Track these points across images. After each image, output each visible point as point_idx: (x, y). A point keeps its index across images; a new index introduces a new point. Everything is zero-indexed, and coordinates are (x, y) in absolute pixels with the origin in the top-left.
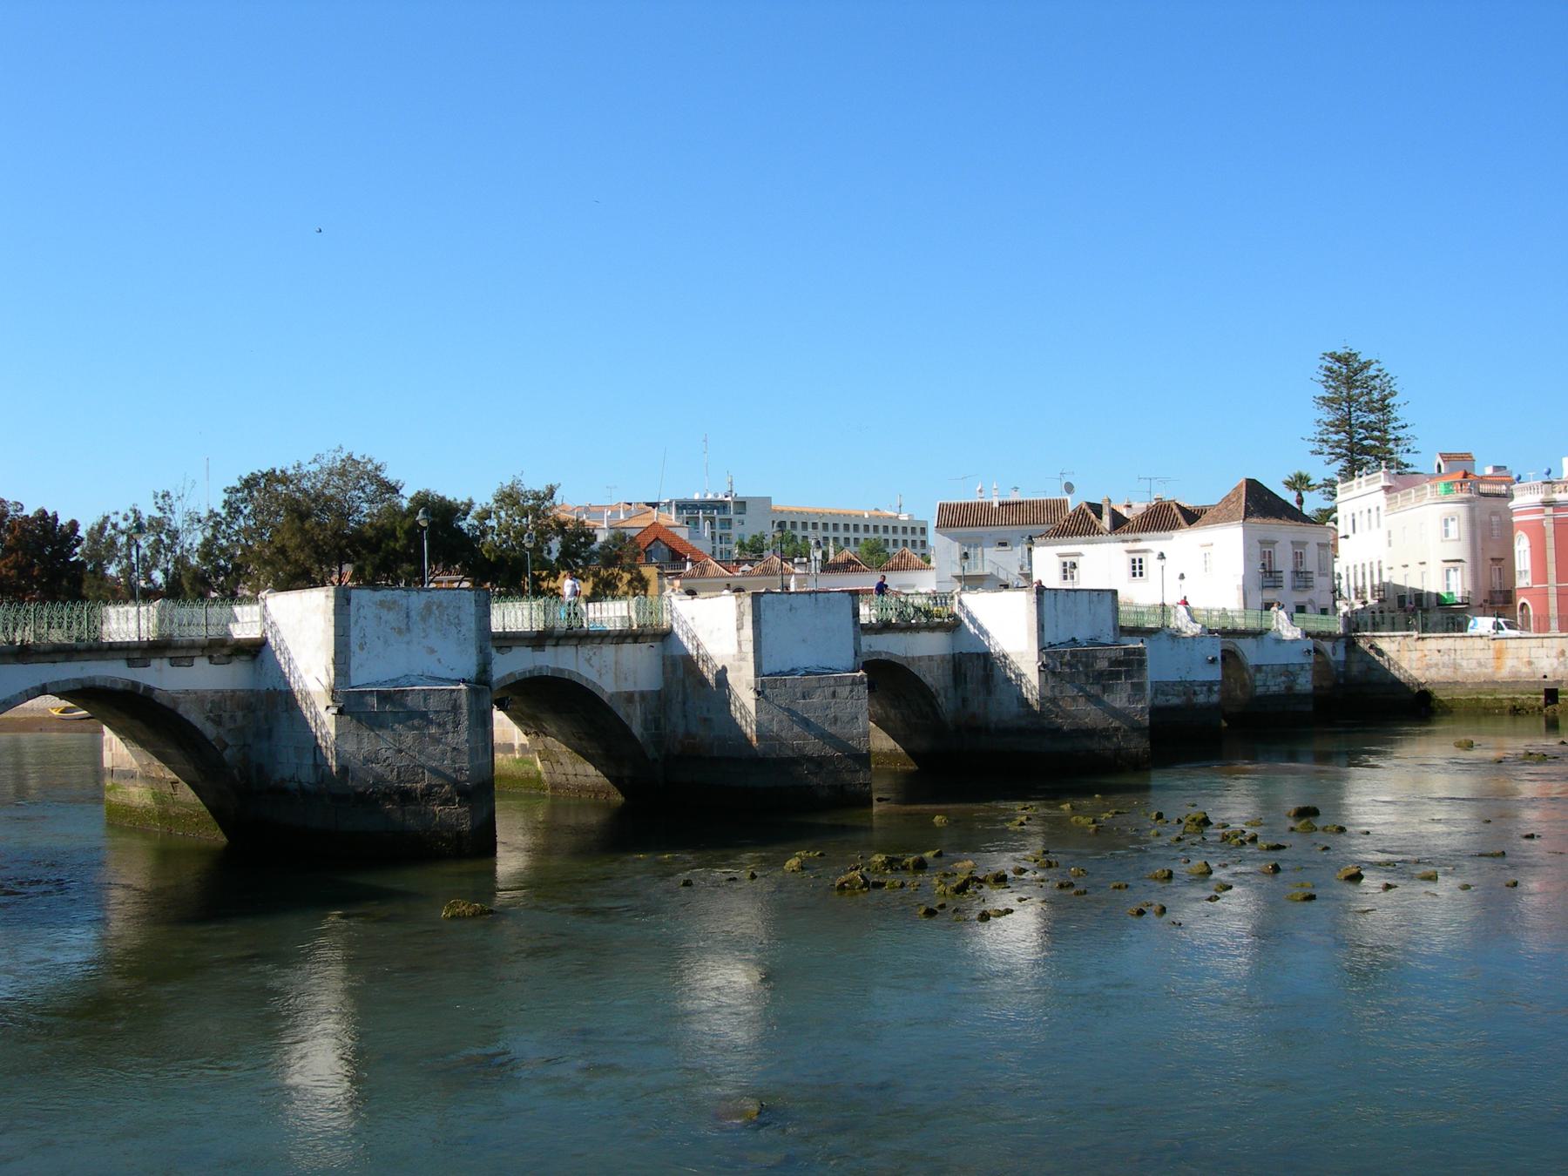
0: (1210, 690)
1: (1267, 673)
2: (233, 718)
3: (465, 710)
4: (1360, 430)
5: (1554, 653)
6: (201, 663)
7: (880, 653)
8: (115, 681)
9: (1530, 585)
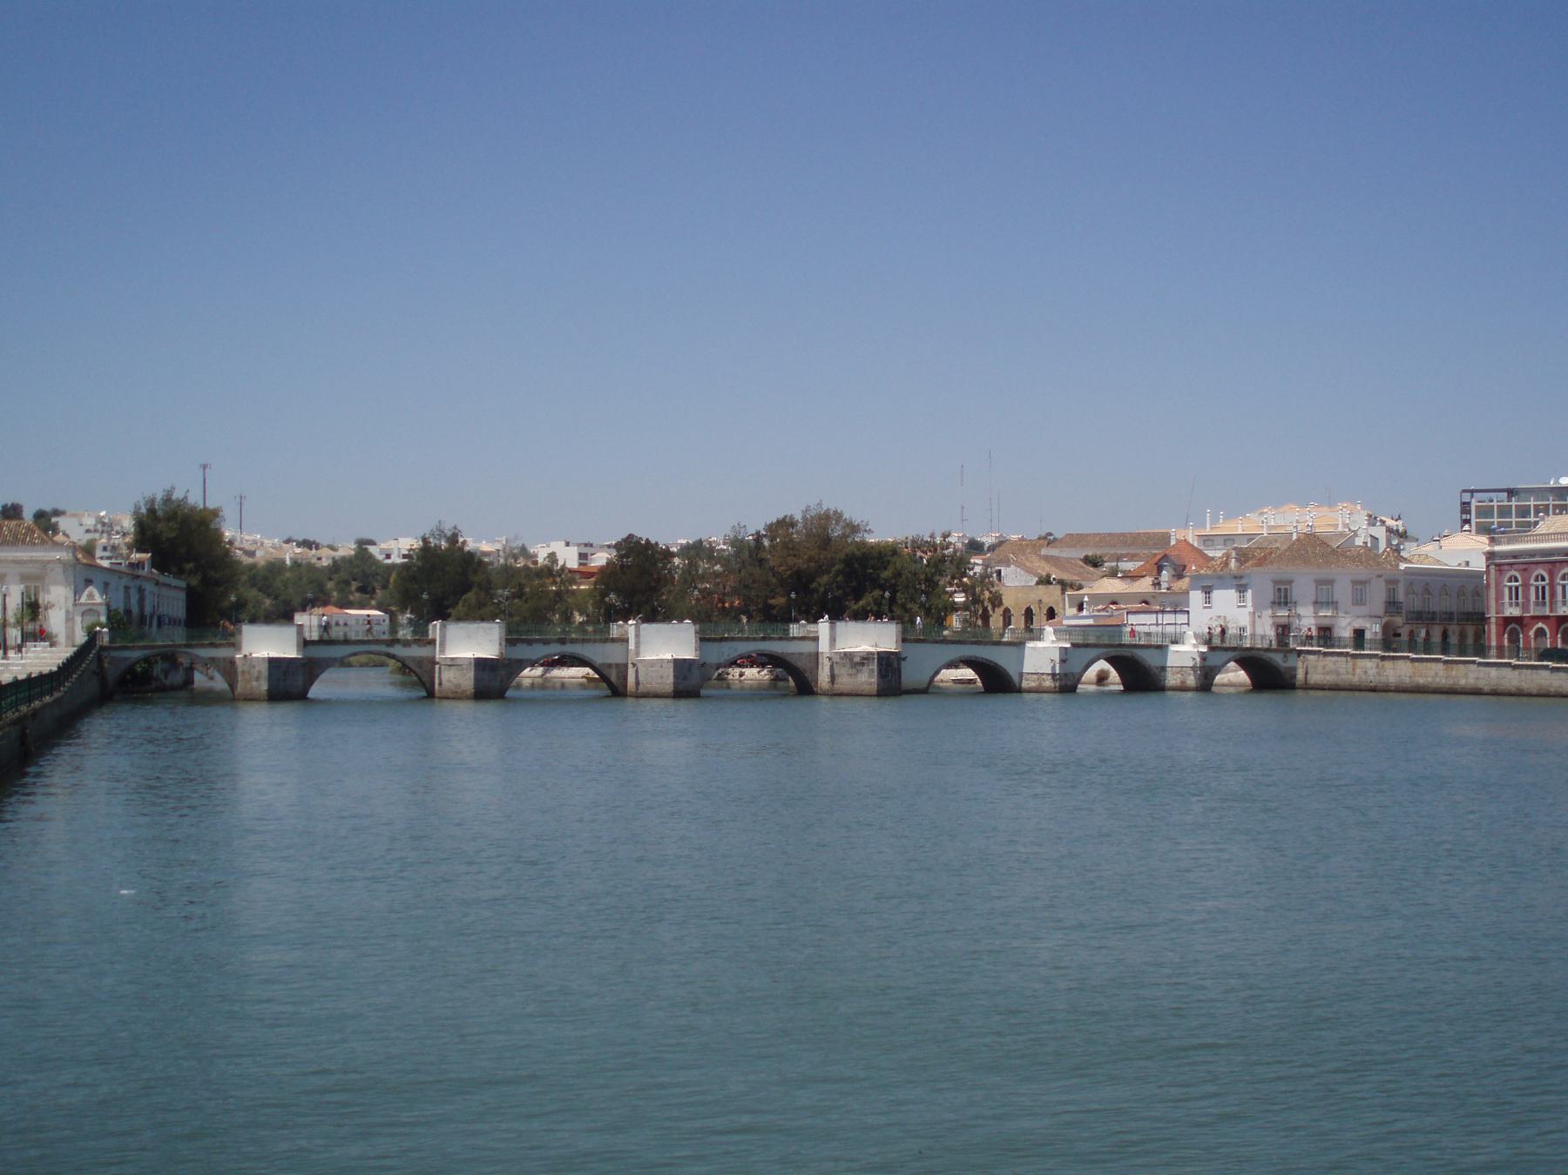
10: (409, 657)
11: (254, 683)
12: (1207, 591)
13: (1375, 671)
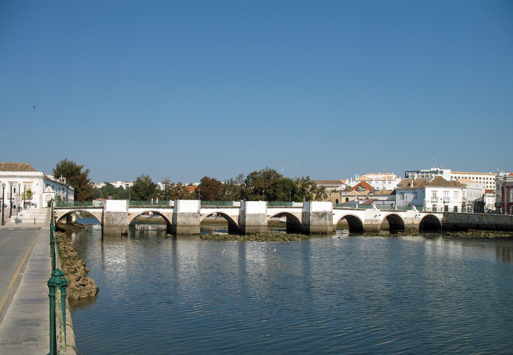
0: (376, 221)
1: (408, 219)
5: (478, 218)
12: (402, 194)
13: (478, 220)
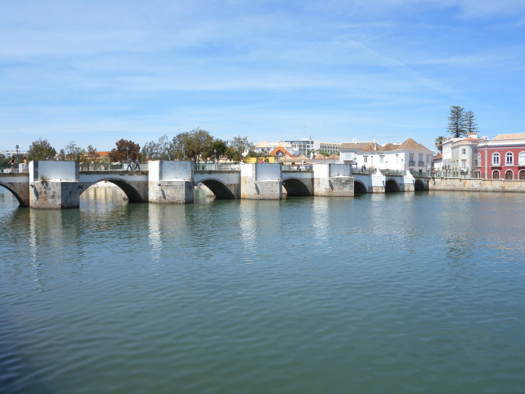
0: (382, 189)
2: (142, 186)
3: (184, 186)
4: (460, 126)
6: (135, 175)
7: (293, 177)
8: (117, 178)
9: (481, 166)
10: (132, 181)
11: (50, 200)
13: (479, 185)
